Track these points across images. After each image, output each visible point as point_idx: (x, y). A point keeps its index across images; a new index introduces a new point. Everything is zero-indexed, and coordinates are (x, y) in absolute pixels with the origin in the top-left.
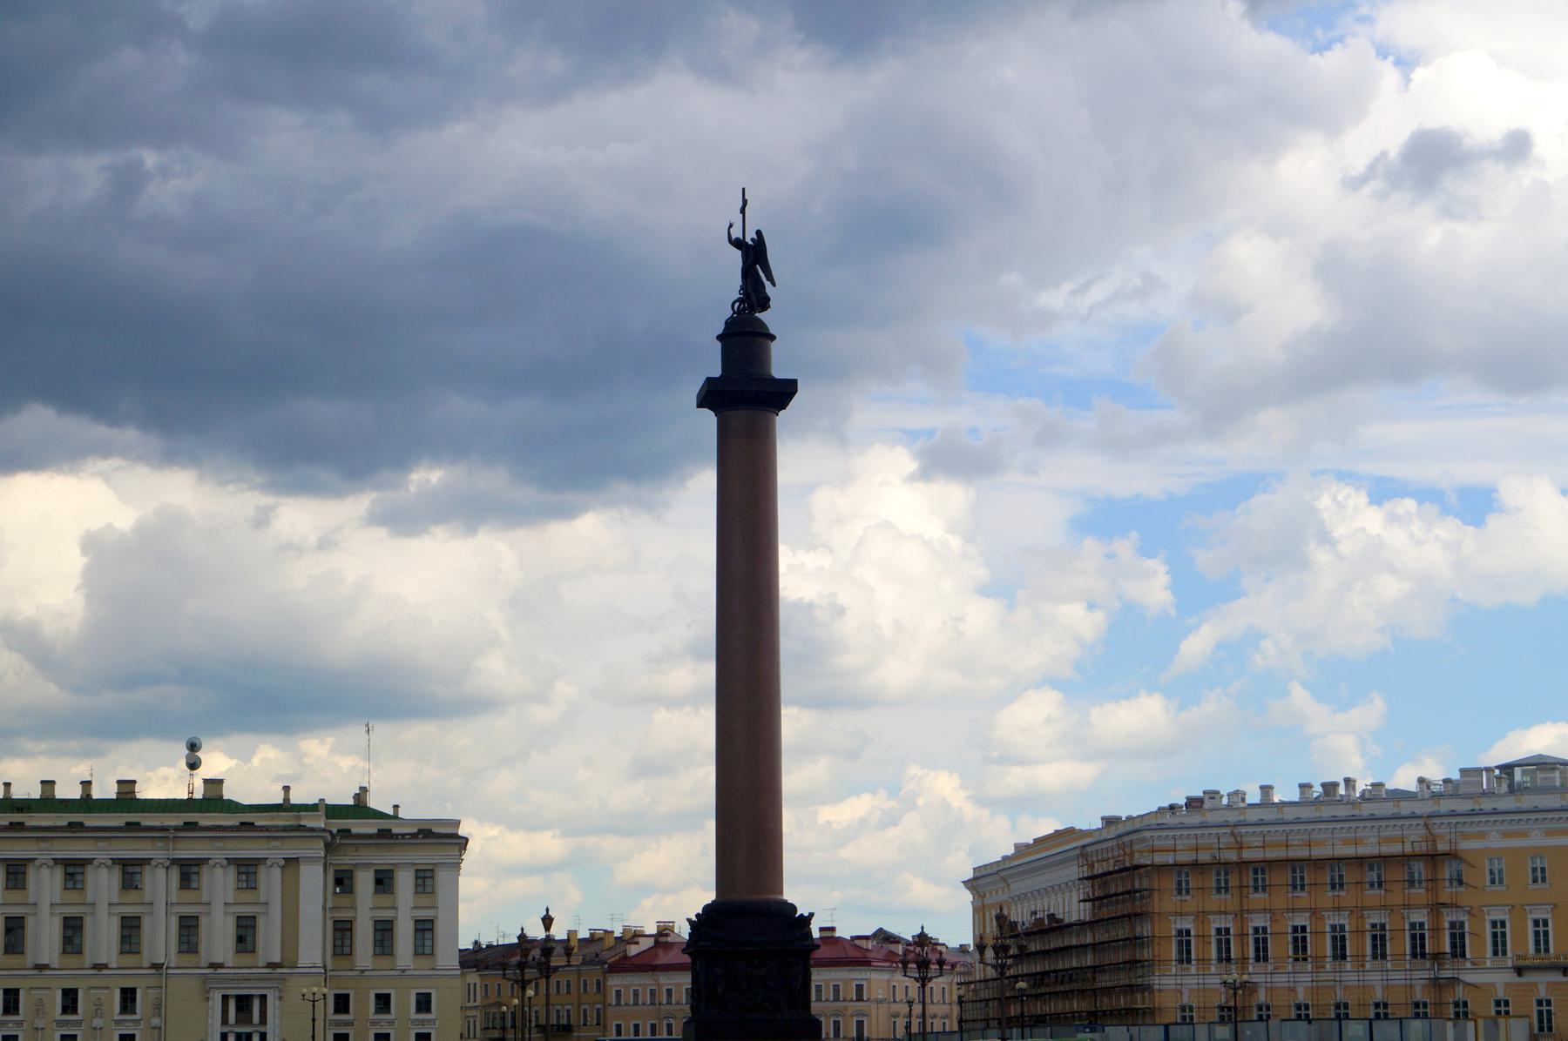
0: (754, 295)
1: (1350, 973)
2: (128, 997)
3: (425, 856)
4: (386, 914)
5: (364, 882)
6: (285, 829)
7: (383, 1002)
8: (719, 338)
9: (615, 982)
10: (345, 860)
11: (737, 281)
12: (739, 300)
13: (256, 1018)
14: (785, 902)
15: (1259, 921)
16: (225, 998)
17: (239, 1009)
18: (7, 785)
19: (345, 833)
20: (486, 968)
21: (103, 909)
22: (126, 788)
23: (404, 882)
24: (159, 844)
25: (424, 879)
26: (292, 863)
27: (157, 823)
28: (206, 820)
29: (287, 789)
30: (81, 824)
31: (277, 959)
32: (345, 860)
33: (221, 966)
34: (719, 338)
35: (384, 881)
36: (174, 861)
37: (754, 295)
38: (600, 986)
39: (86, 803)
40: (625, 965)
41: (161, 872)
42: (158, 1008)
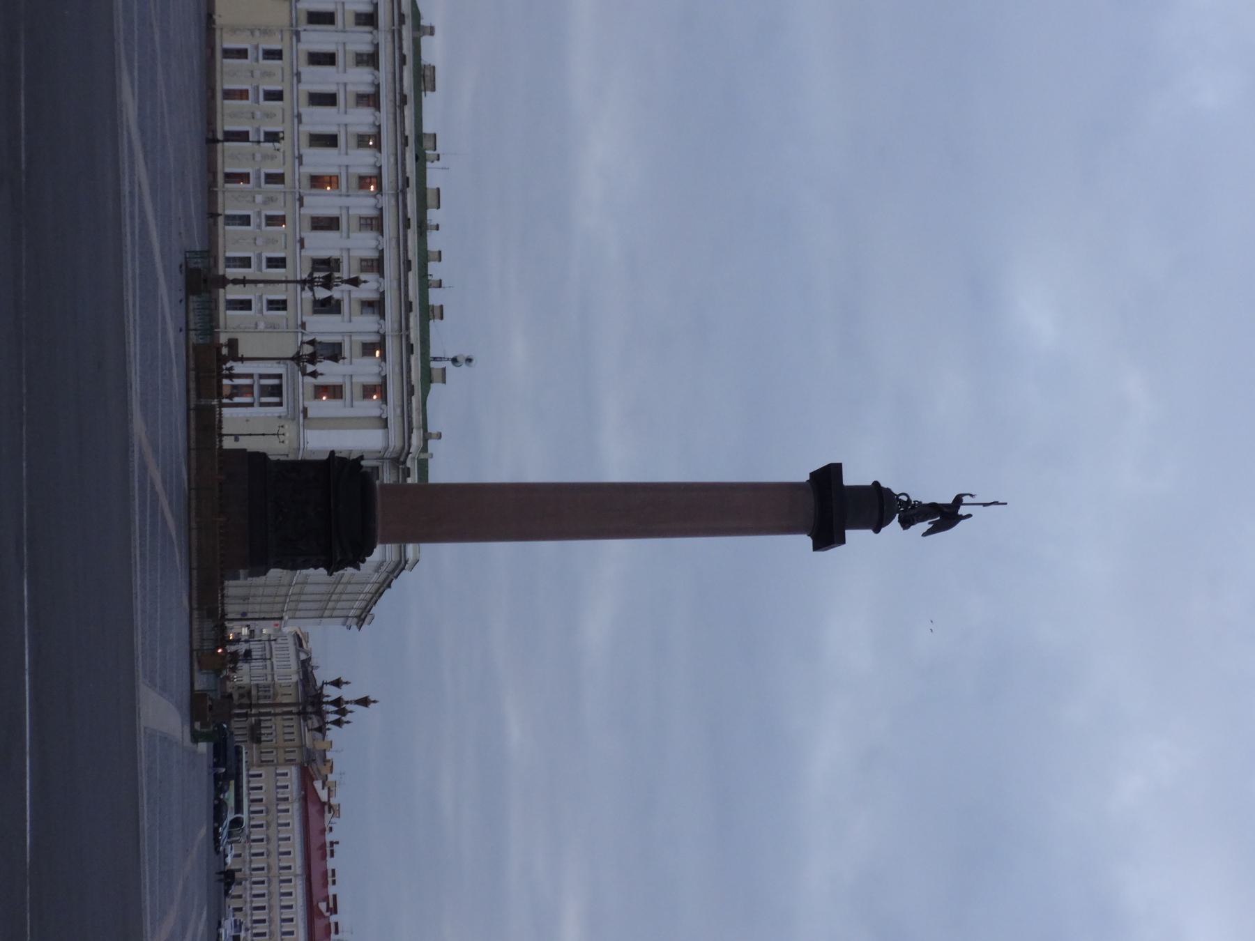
0: (911, 513)
6: (410, 417)
8: (876, 484)
9: (293, 772)
11: (926, 501)
12: (909, 501)
13: (264, 400)
16: (279, 376)
17: (272, 386)
18: (437, 227)
20: (304, 686)
22: (437, 312)
24: (396, 326)
26: (384, 423)
27: (412, 324)
30: (410, 269)
31: (310, 414)
34: (876, 484)
36: (383, 337)
37: (911, 513)
38: (289, 762)
39: (425, 283)
40: (306, 778)
41: (375, 327)
42: (272, 327)
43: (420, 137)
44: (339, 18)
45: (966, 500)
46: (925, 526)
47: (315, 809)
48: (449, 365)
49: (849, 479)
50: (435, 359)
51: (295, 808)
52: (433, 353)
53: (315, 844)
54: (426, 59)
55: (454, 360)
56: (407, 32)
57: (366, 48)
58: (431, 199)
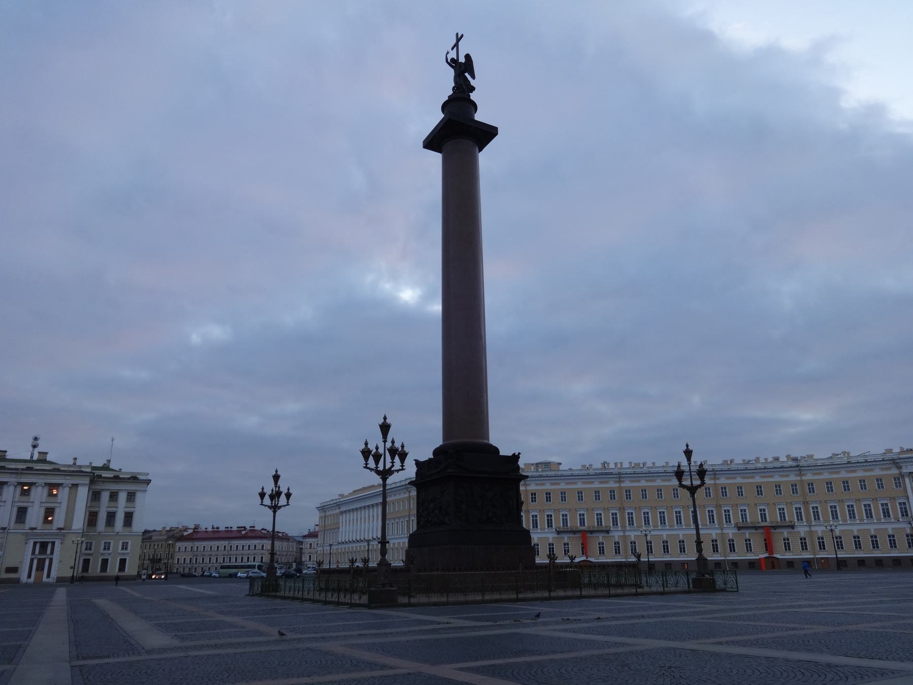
3: (132, 487)
4: (113, 510)
5: (105, 496)
6: (73, 472)
7: (107, 547)
9: (178, 544)
10: (98, 487)
13: (49, 552)
14: (491, 445)
16: (35, 543)
17: (41, 547)
19: (100, 476)
23: (122, 497)
25: (131, 496)
29: (75, 459)
32: (98, 487)
33: (35, 529)
35: (114, 496)
38: (173, 546)
40: (182, 538)
41: (12, 488)
45: (453, 55)
47: (197, 535)
50: (32, 457)
51: (197, 544)
52: (28, 458)
53: (212, 536)
55: (34, 447)
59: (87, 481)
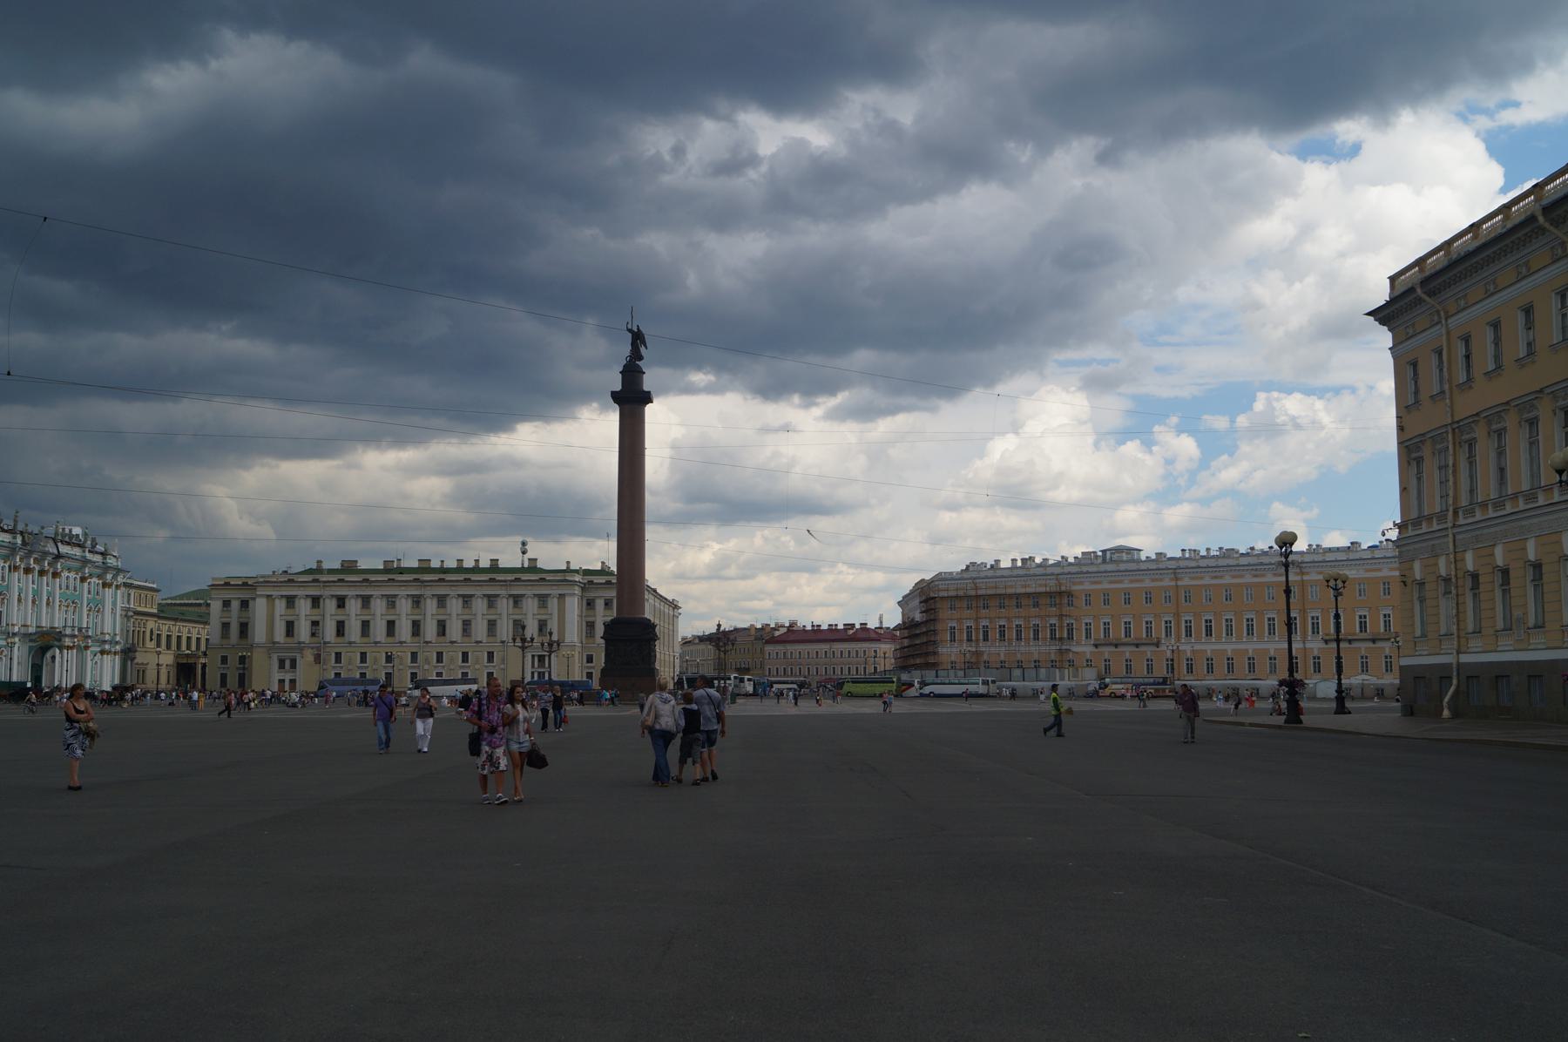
0: (636, 355)
1: (1022, 647)
2: (491, 656)
9: (768, 648)
10: (591, 595)
15: (984, 623)
19: (591, 582)
21: (479, 617)
26: (562, 596)
28: (525, 577)
37: (636, 355)
38: (762, 651)
39: (476, 569)
40: (773, 641)
43: (386, 571)
44: (315, 618)
46: (643, 349)
48: (527, 556)
49: (618, 387)
54: (337, 566)
56: (324, 578)
57: (334, 602)
58: (425, 565)
59: (577, 591)
